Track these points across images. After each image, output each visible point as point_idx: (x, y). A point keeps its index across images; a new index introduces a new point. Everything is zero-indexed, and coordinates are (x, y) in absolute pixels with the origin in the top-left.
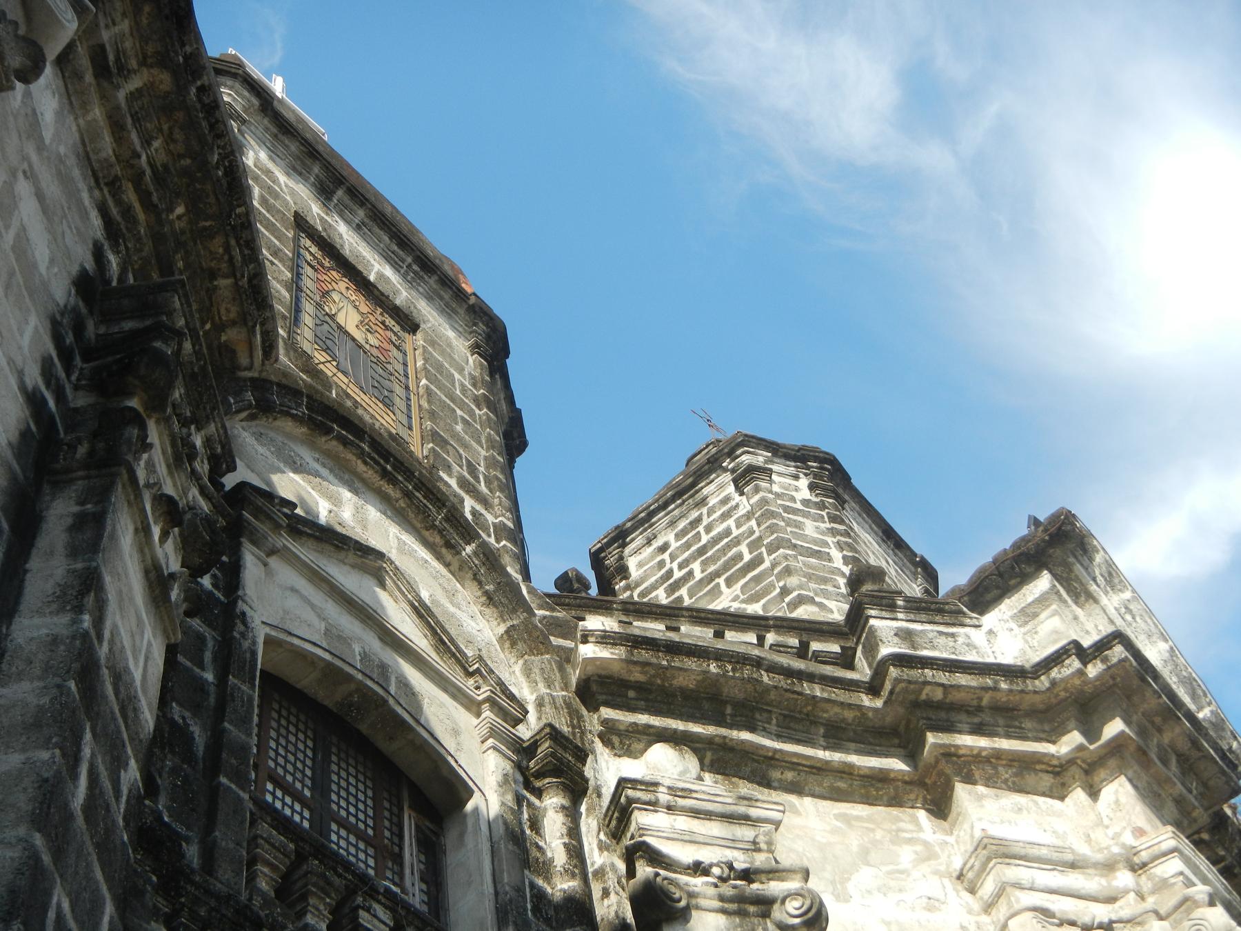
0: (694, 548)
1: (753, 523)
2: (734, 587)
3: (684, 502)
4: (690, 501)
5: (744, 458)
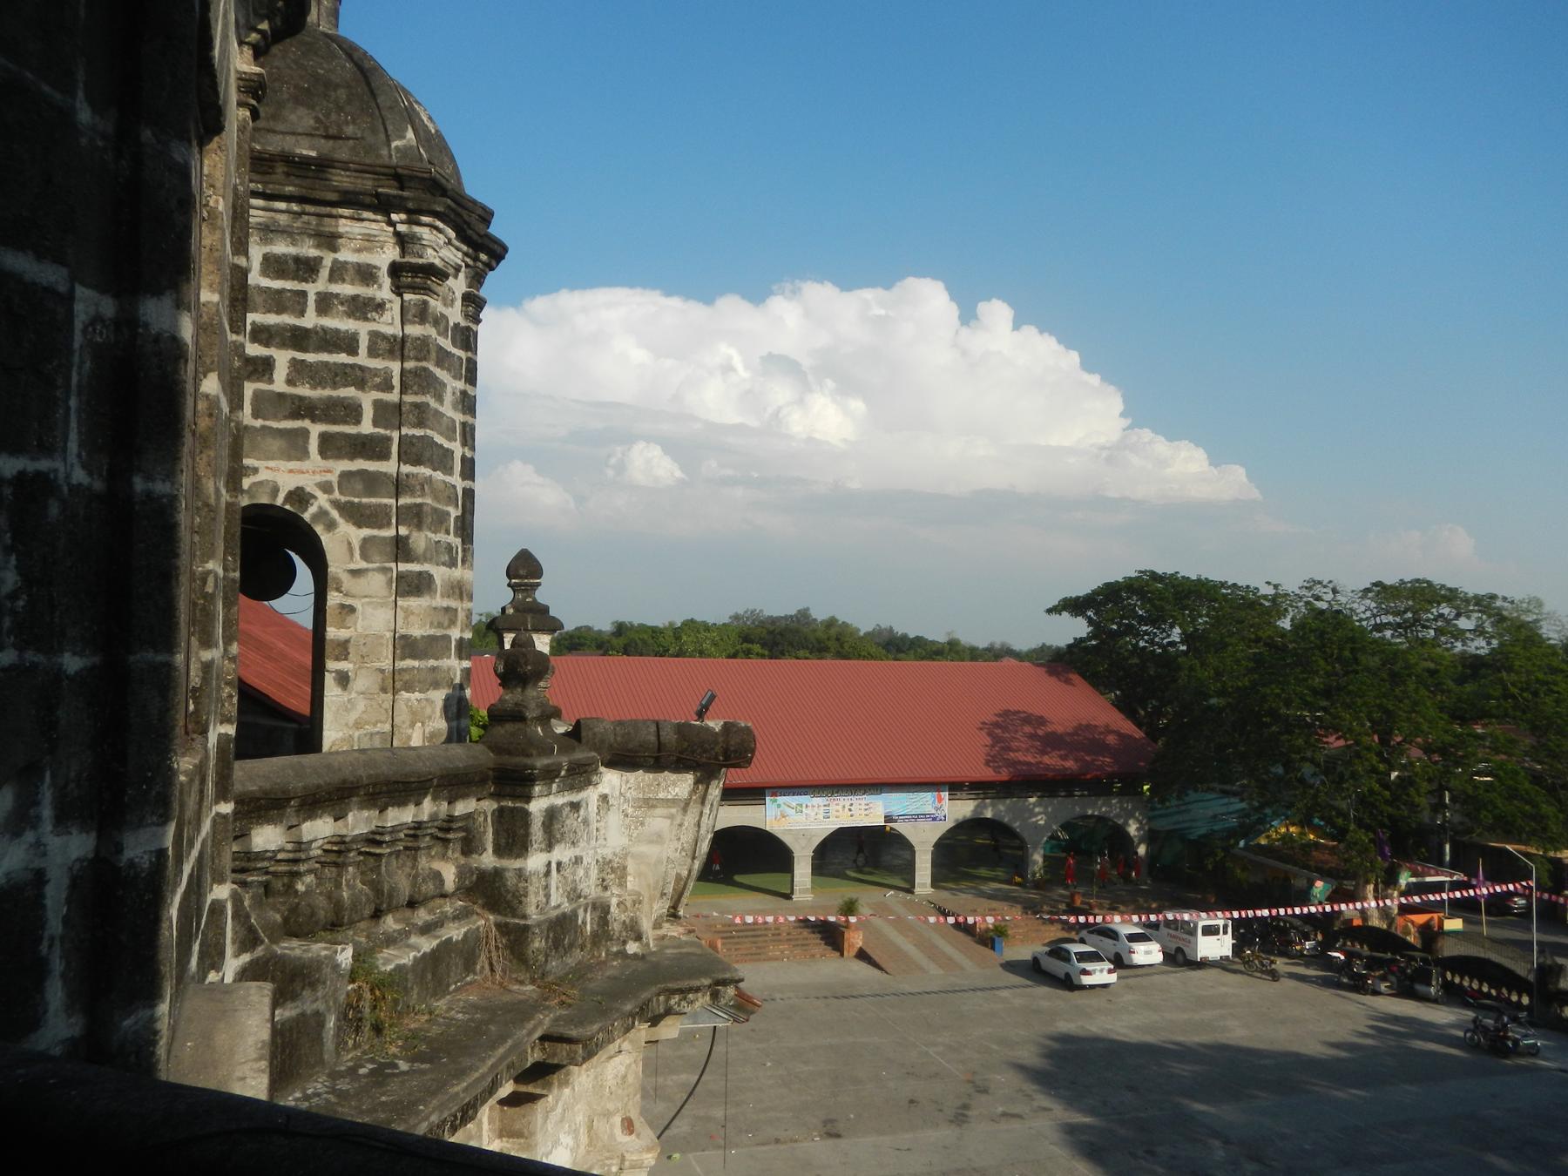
0: (287, 319)
1: (395, 367)
2: (330, 464)
3: (303, 213)
4: (314, 221)
5: (424, 232)
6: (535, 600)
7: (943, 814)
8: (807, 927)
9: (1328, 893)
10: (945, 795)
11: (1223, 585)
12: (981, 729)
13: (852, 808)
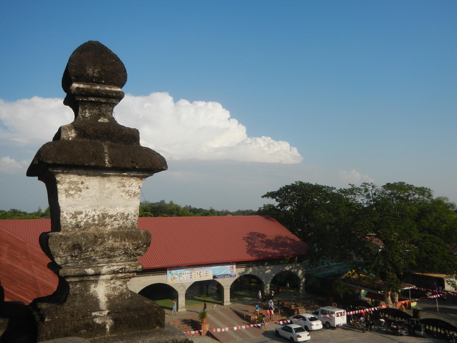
6: (112, 120)
7: (234, 274)
8: (186, 323)
9: (366, 294)
10: (234, 266)
11: (324, 187)
12: (243, 240)
13: (201, 273)
